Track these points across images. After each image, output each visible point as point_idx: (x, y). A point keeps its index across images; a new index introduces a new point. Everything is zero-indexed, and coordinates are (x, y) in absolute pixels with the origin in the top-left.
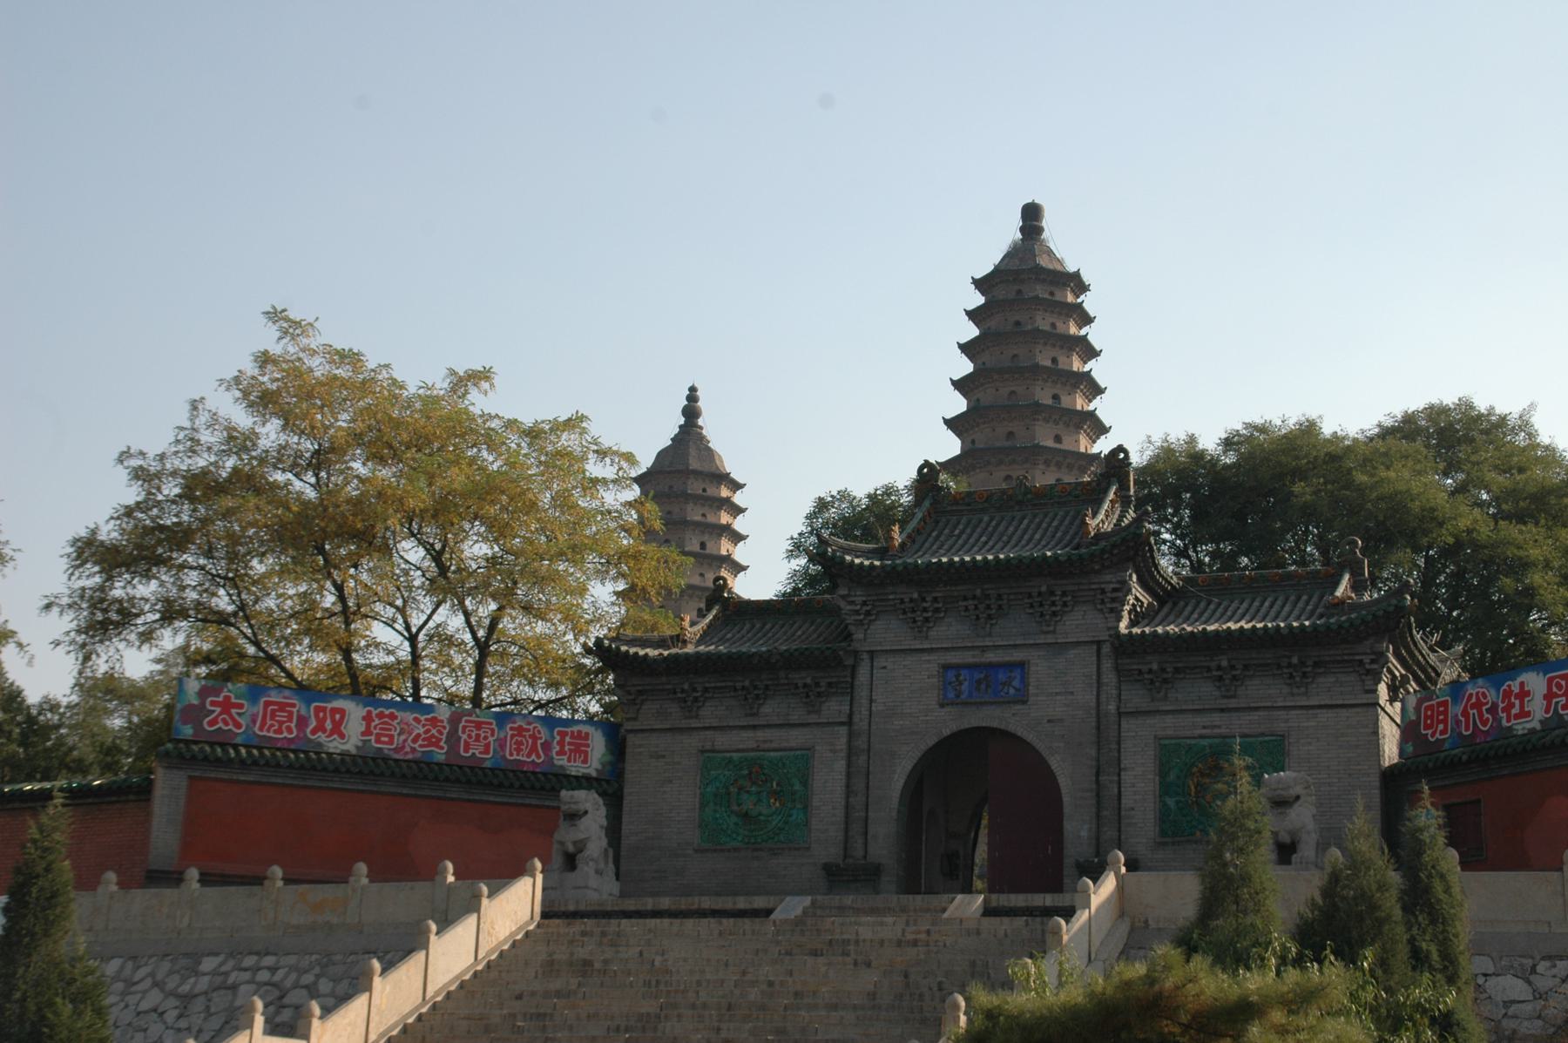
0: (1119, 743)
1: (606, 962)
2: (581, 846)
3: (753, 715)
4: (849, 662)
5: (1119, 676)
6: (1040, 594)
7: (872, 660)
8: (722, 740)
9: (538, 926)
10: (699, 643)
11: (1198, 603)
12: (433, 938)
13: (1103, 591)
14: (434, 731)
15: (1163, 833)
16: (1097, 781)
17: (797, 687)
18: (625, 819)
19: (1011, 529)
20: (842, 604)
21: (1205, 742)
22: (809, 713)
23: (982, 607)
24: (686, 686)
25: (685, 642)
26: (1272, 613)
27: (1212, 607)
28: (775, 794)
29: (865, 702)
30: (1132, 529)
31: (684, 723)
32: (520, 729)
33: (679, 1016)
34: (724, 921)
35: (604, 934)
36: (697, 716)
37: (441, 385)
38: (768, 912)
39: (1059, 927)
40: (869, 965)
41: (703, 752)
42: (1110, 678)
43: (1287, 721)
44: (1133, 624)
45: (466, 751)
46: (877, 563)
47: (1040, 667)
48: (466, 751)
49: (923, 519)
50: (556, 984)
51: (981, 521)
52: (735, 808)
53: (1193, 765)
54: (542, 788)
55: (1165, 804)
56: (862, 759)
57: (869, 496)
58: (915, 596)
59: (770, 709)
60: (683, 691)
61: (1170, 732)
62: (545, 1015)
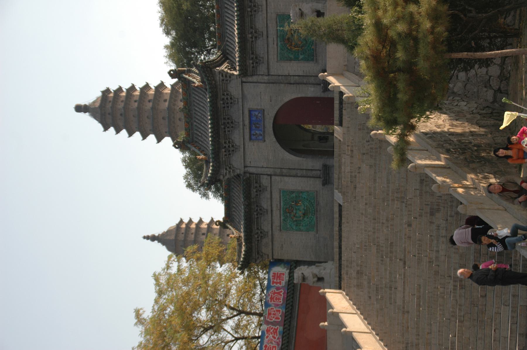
0: (279, 76)
1: (357, 266)
2: (315, 275)
3: (267, 212)
4: (248, 175)
5: (255, 75)
6: (224, 104)
7: (247, 167)
8: (277, 223)
9: (344, 291)
10: (240, 231)
11: (228, 45)
12: (348, 330)
13: (223, 80)
14: (272, 331)
15: (313, 60)
16: (294, 84)
17: (257, 195)
18: (305, 259)
19: (199, 114)
20: (226, 177)
21: (279, 44)
22: (267, 190)
23: (228, 125)
24: (256, 236)
25: (240, 237)
26: (232, 17)
27: (229, 40)
28: (297, 203)
29: (263, 169)
30: (200, 69)
31: (270, 237)
32: (271, 298)
33: (377, 238)
34: (343, 221)
35: (347, 266)
36: (267, 232)
37: (141, 328)
38: (340, 206)
39: (346, 97)
40: (360, 168)
41: (280, 230)
42: (255, 78)
43: (272, 13)
44: (235, 69)
45: (279, 319)
46: (211, 164)
47: (251, 104)
48: (279, 319)
49: (195, 147)
50: (365, 283)
51: (196, 126)
52: (301, 218)
53: (287, 48)
54: (293, 290)
55: (302, 59)
56: (284, 171)
57: (186, 168)
58: (224, 150)
59: (265, 205)
60: (258, 237)
61: (275, 56)
62: (377, 288)
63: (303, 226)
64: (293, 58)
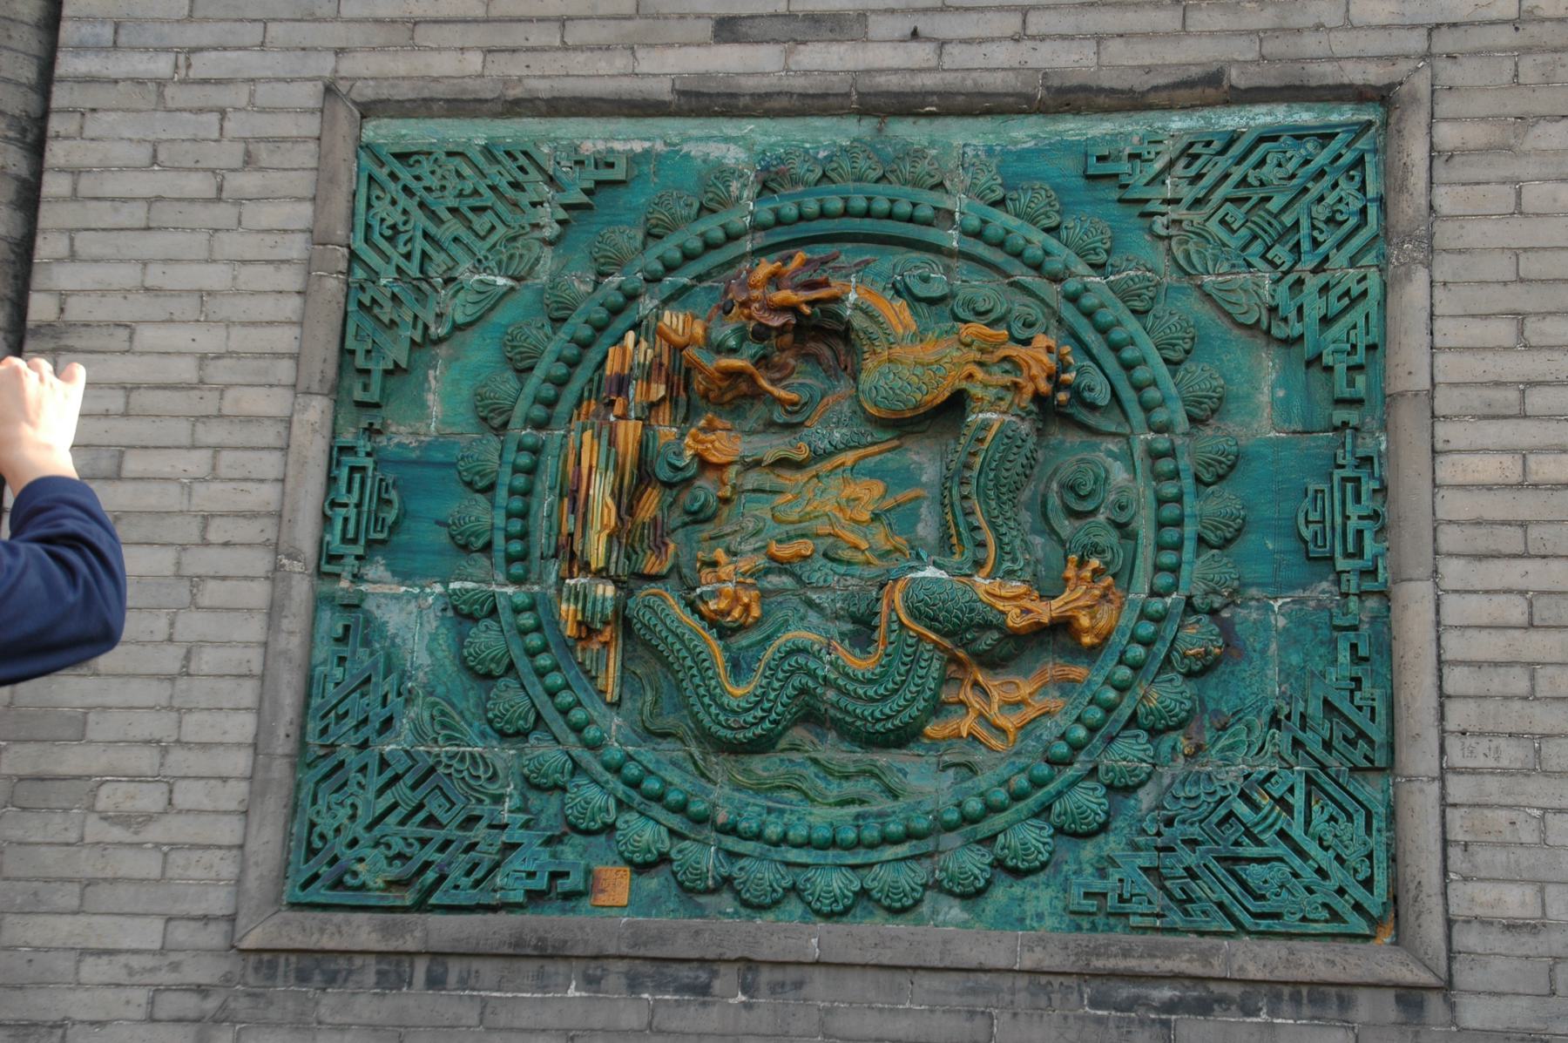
15: (317, 875)
21: (729, 146)
55: (354, 624)
61: (452, 64)
64: (401, 435)
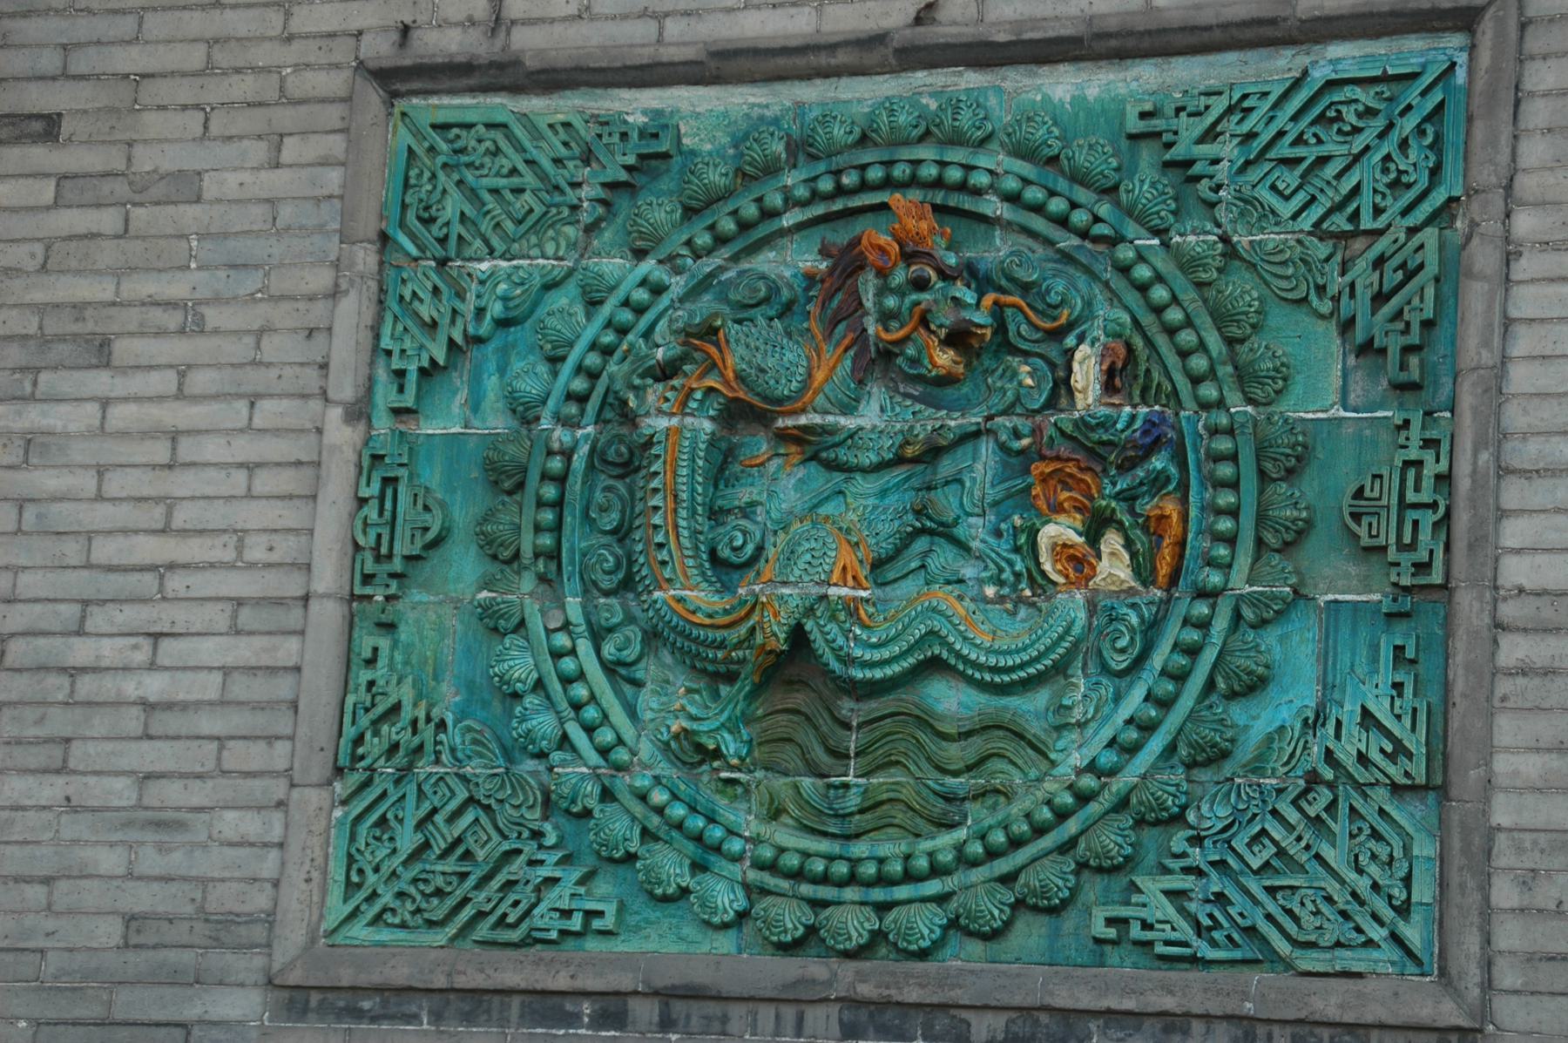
41: (394, 80)
63: (497, 624)
